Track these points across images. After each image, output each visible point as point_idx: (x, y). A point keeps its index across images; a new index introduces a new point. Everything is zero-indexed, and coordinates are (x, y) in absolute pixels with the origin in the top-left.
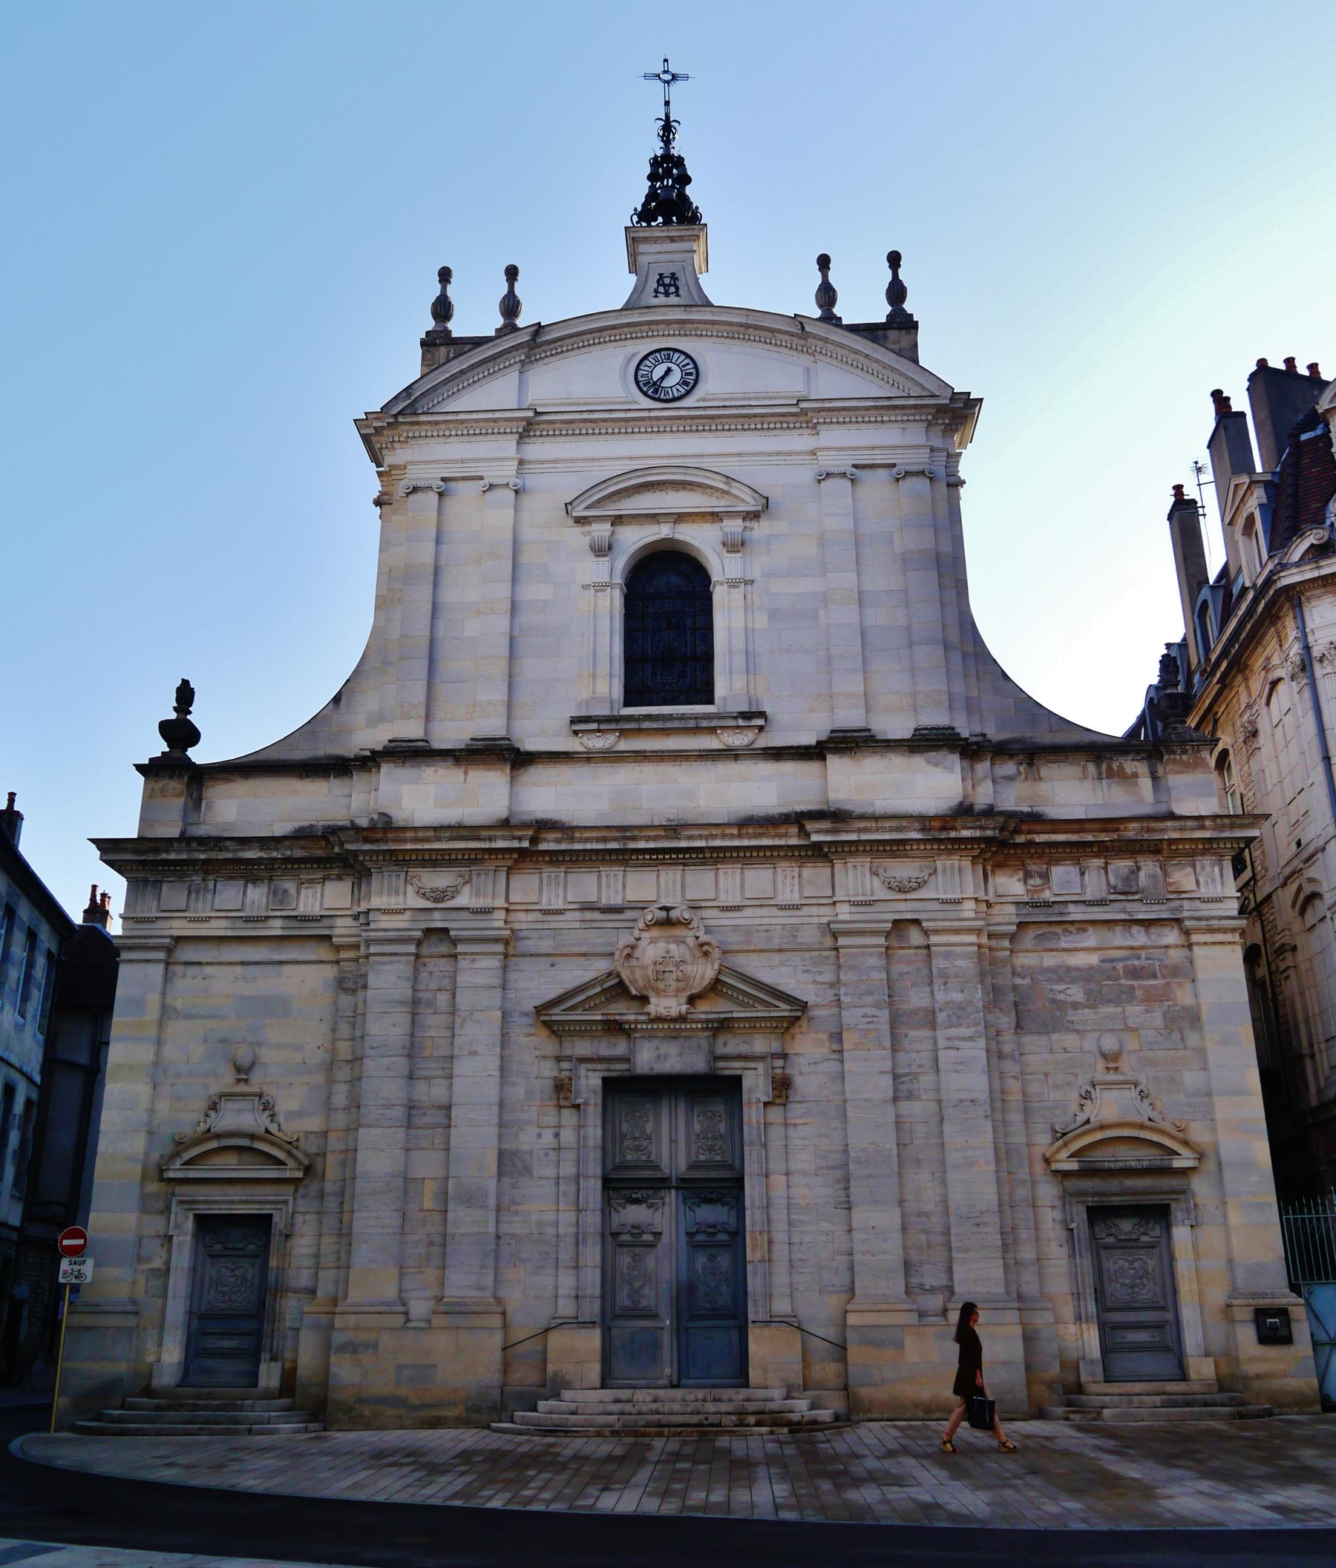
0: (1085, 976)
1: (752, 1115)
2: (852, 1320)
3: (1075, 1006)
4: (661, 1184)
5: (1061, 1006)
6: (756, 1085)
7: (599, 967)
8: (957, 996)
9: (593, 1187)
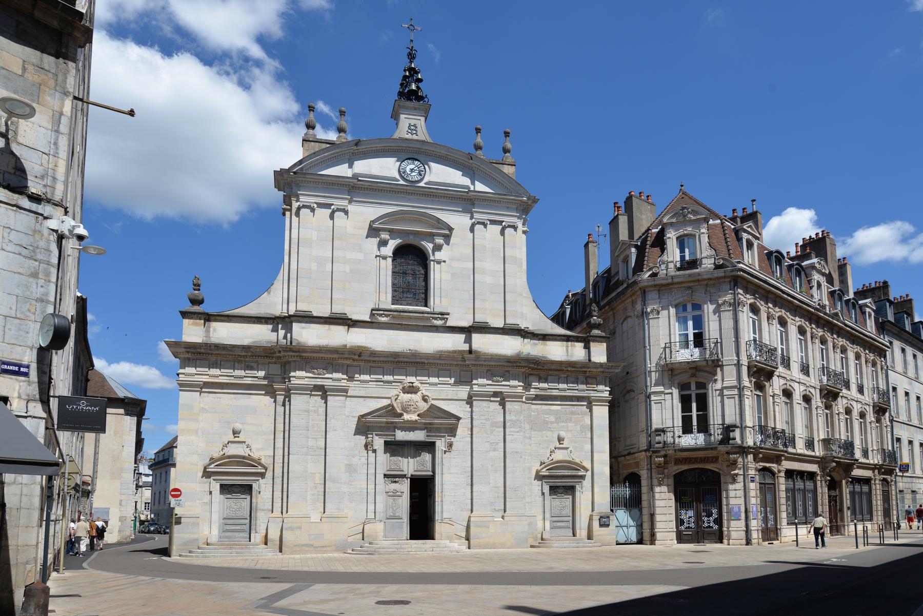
0: (555, 413)
1: (438, 454)
2: (472, 519)
3: (552, 423)
4: (404, 476)
5: (546, 422)
6: (440, 445)
7: (386, 402)
8: (514, 418)
9: (380, 477)
